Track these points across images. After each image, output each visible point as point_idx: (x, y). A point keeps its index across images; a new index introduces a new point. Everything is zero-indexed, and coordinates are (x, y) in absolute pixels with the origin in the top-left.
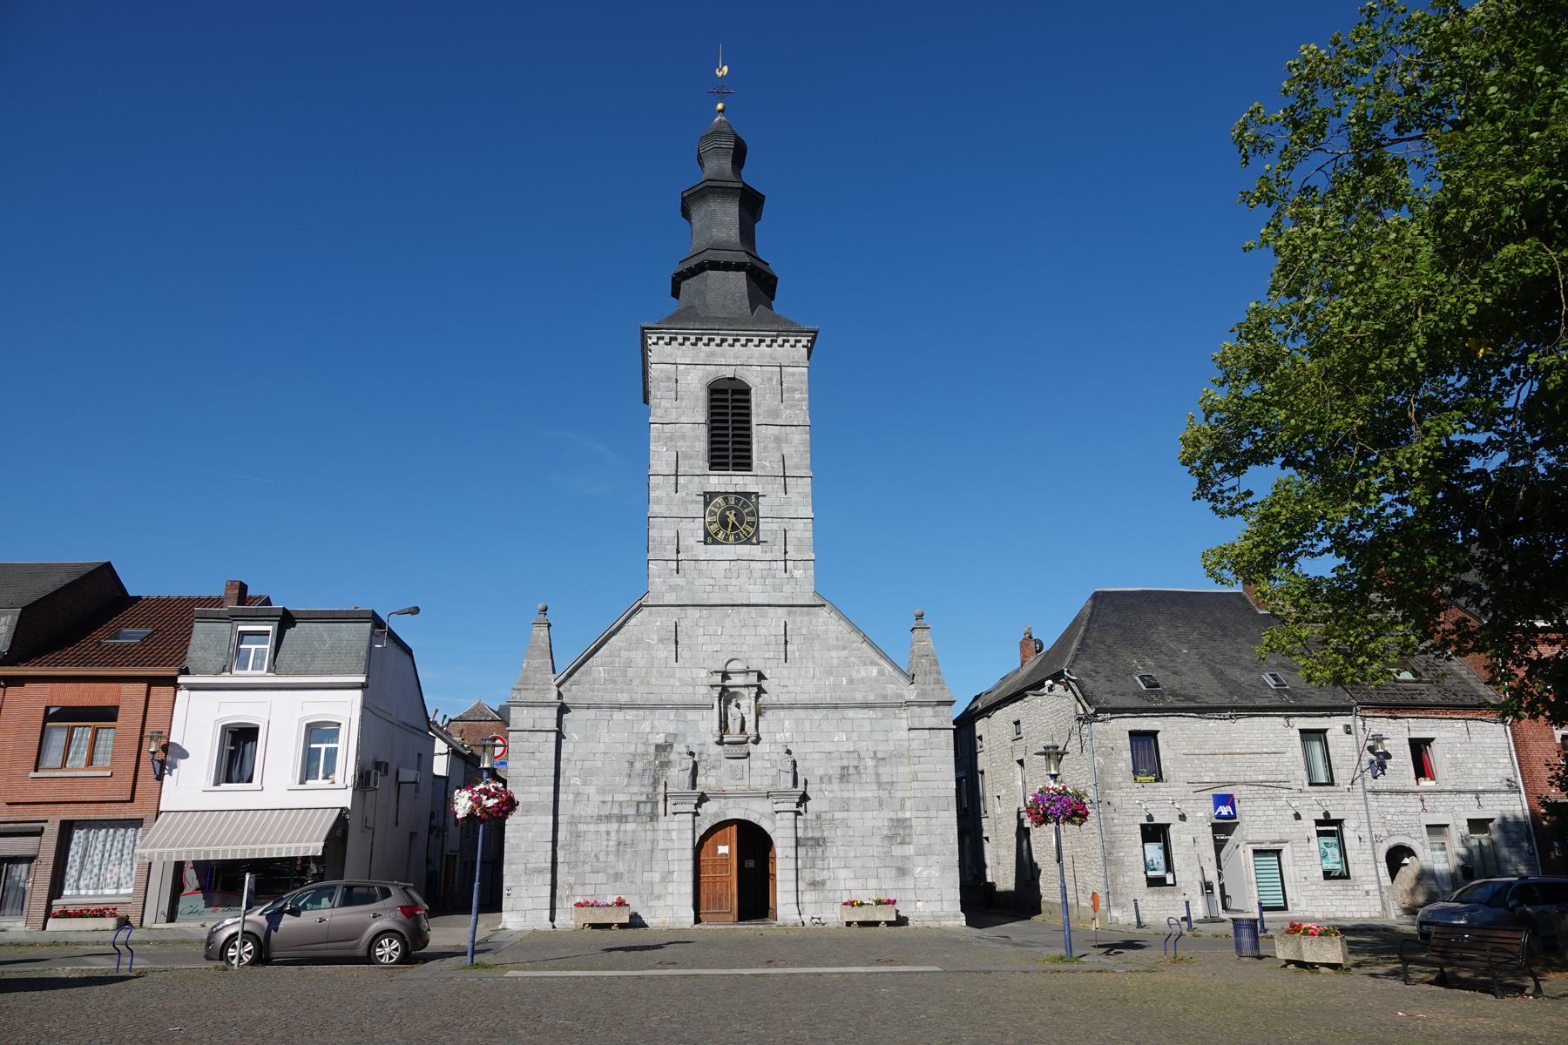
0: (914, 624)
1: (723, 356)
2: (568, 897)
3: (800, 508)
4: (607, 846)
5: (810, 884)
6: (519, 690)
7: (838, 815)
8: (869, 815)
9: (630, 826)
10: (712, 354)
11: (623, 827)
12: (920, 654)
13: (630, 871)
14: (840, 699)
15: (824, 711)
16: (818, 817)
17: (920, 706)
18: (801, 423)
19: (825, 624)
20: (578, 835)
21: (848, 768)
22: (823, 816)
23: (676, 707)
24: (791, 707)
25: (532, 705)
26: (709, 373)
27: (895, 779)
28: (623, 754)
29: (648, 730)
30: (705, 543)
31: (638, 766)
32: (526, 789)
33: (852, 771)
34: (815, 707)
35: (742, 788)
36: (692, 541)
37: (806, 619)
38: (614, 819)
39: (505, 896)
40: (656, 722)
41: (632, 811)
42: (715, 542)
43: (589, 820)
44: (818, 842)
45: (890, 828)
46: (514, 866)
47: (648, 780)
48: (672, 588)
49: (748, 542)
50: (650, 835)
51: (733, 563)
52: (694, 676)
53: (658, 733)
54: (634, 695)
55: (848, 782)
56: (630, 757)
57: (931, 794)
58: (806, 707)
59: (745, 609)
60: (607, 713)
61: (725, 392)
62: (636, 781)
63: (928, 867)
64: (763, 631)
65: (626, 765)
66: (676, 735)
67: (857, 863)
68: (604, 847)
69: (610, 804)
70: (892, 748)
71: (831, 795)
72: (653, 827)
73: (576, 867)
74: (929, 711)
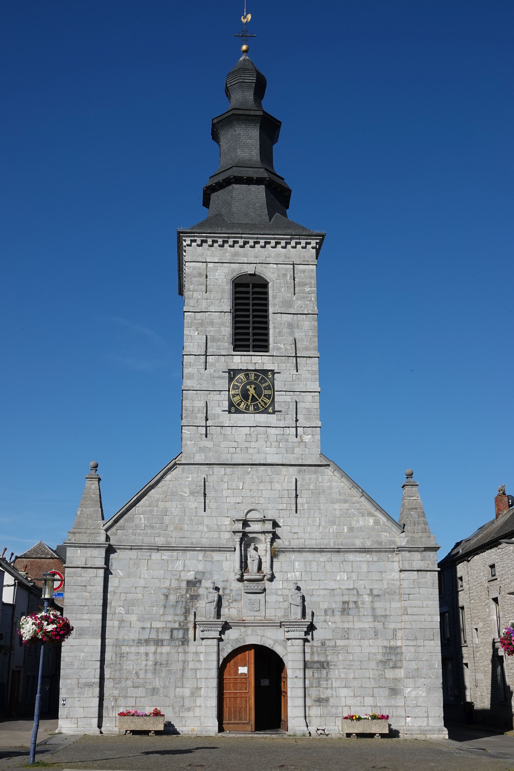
0: (404, 481)
1: (246, 256)
2: (113, 707)
3: (309, 383)
4: (146, 665)
5: (316, 701)
6: (74, 533)
7: (339, 643)
8: (366, 643)
9: (165, 649)
10: (236, 254)
11: (159, 650)
12: (410, 507)
13: (165, 687)
14: (342, 545)
15: (329, 554)
16: (323, 644)
17: (410, 551)
18: (310, 312)
19: (330, 481)
20: (122, 656)
21: (348, 603)
22: (327, 643)
23: (204, 549)
24: (300, 550)
25: (85, 546)
26: (233, 270)
27: (388, 613)
28: (160, 588)
29: (181, 568)
30: (230, 412)
31: (172, 598)
32: (79, 616)
33: (351, 605)
34: (321, 551)
35: (259, 618)
36: (218, 411)
37: (313, 476)
38: (152, 643)
39: (60, 706)
40: (187, 562)
41: (167, 636)
42: (238, 411)
43: (131, 643)
44: (323, 665)
45: (384, 654)
46: (69, 681)
47: (180, 611)
48: (202, 450)
49: (265, 411)
50: (181, 657)
51: (252, 429)
52: (219, 524)
53: (189, 571)
54: (169, 539)
55: (348, 614)
56: (165, 591)
57: (419, 626)
58: (313, 550)
59: (262, 468)
60: (147, 553)
61: (247, 285)
62: (171, 611)
63: (416, 688)
64: (277, 486)
65: (162, 597)
66: (203, 573)
67: (356, 683)
68: (143, 666)
69: (148, 631)
70: (385, 586)
71: (334, 626)
72: (184, 650)
73: (120, 682)
74: (417, 556)
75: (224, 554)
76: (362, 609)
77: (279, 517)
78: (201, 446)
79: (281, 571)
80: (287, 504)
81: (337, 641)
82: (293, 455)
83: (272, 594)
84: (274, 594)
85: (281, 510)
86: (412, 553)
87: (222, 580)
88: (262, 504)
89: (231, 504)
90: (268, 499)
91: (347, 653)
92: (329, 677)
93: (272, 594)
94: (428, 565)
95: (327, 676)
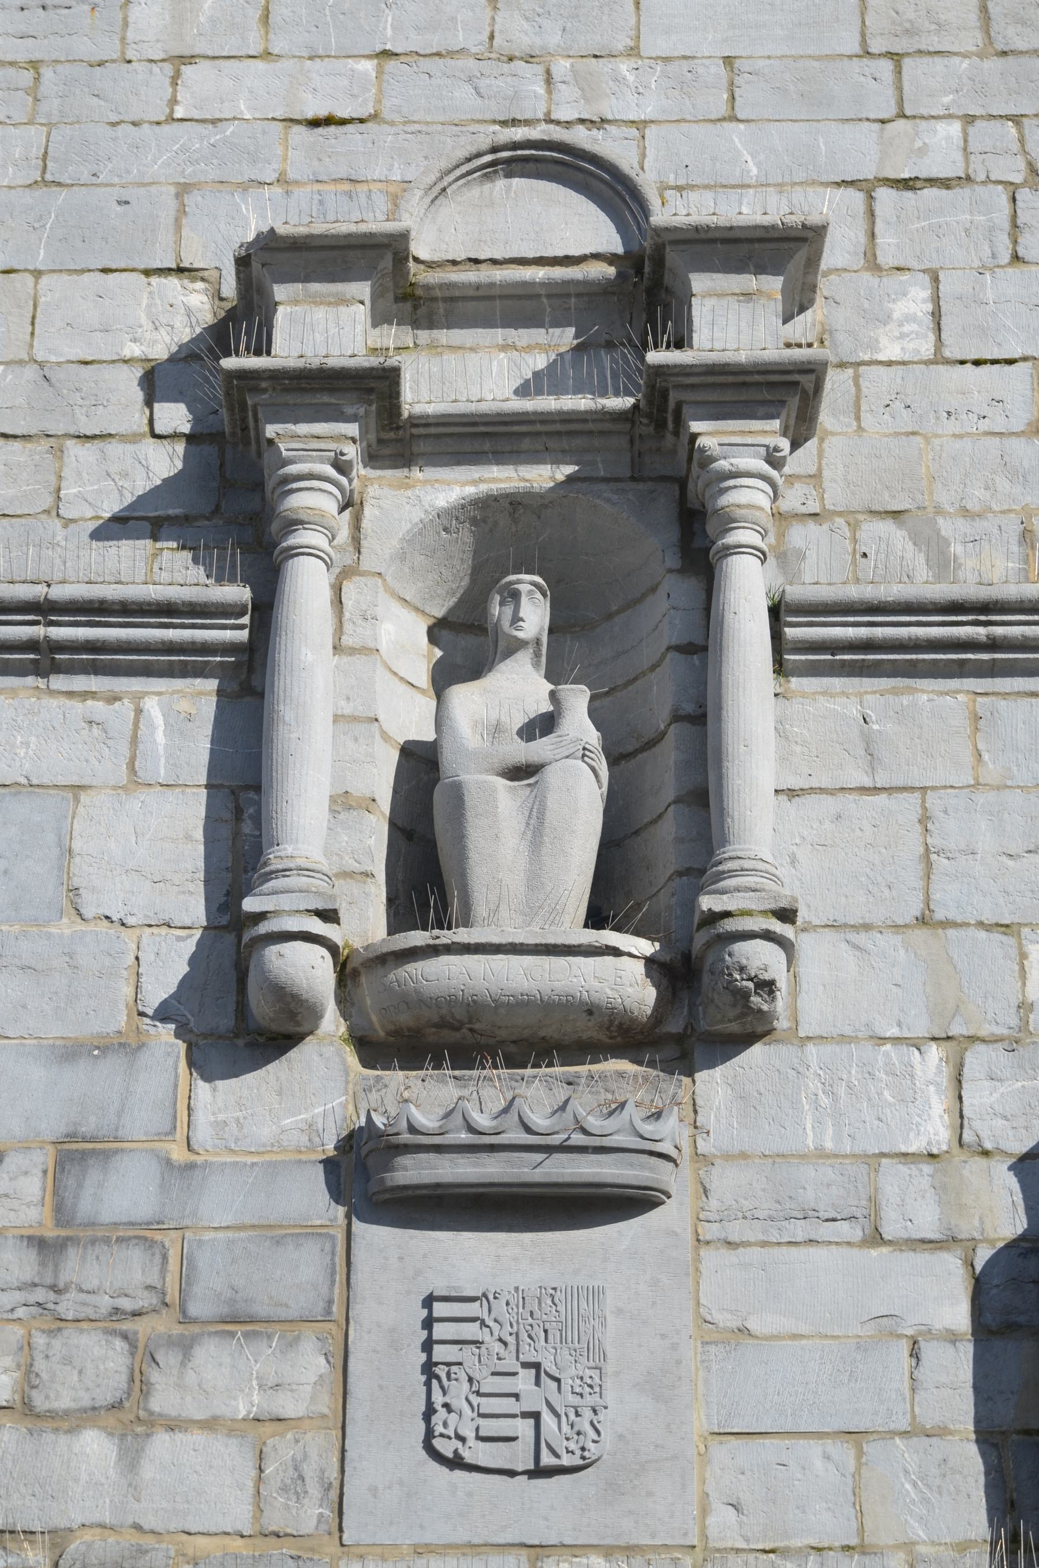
75: (114, 698)
77: (873, 265)
79: (923, 921)
80: (969, 120)
83: (800, 1230)
84: (826, 1231)
85: (907, 184)
87: (55, 1030)
88: (641, 125)
89: (230, 129)
90: (719, 69)
93: (800, 1230)
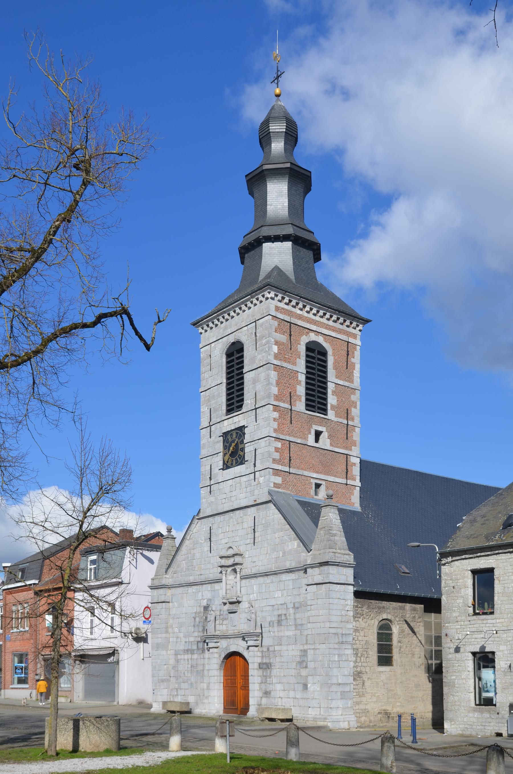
2: (176, 695)
9: (195, 656)
15: (271, 577)
16: (268, 649)
17: (312, 568)
29: (201, 598)
31: (197, 619)
33: (283, 617)
41: (195, 647)
53: (204, 599)
55: (281, 625)
62: (196, 629)
76: (289, 620)
78: (210, 502)
81: (275, 647)
82: (253, 497)
86: (314, 569)
91: (281, 656)
92: (271, 675)
94: (324, 578)
95: (270, 674)
